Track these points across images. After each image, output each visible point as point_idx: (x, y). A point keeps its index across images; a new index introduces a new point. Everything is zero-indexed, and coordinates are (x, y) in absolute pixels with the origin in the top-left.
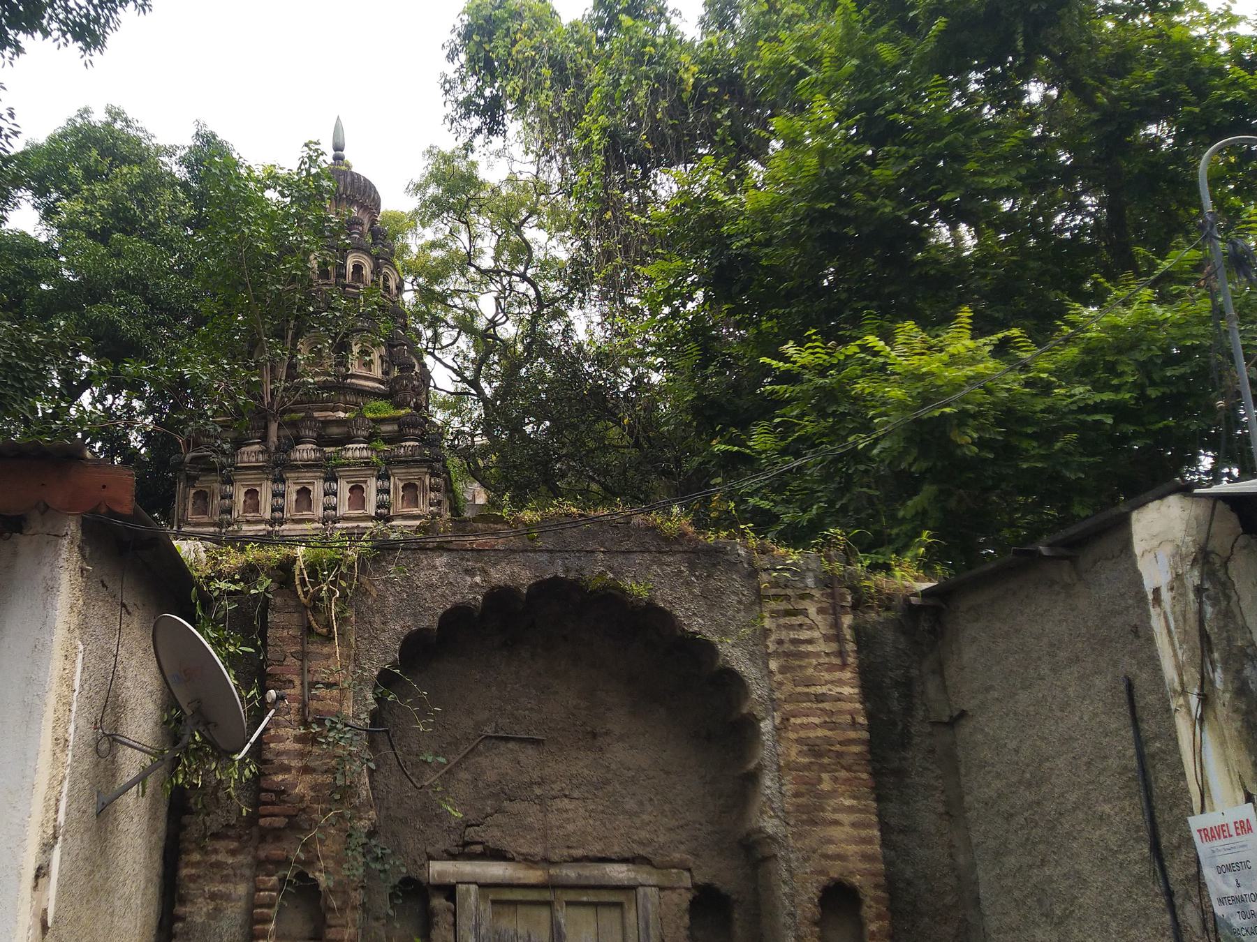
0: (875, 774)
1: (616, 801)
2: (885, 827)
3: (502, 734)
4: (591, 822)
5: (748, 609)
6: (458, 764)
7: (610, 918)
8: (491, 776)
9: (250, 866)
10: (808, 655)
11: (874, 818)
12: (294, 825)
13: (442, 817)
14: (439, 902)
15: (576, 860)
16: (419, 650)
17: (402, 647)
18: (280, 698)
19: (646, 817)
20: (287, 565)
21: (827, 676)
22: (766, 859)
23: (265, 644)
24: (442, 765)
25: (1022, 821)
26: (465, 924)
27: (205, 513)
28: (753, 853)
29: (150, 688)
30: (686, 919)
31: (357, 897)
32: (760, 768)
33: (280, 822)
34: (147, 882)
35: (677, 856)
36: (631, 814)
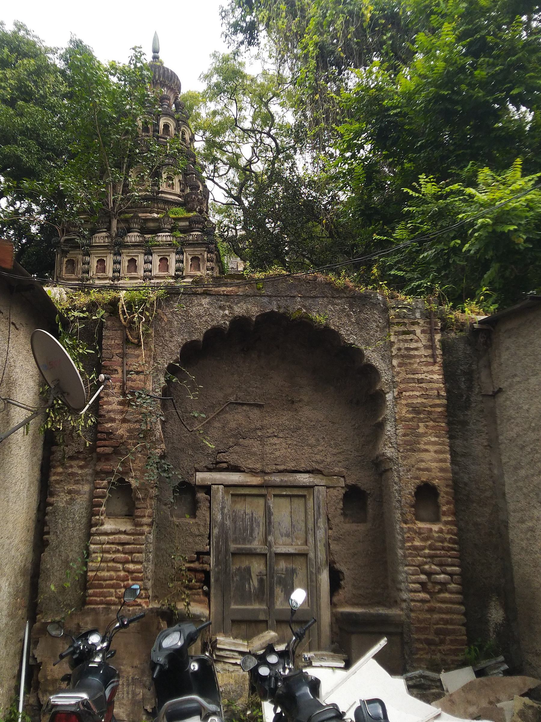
1: (304, 439)
2: (453, 453)
3: (239, 401)
4: (289, 450)
6: (214, 418)
7: (298, 503)
8: (233, 425)
9: (91, 475)
11: (448, 448)
12: (117, 452)
13: (204, 448)
14: (201, 495)
15: (280, 472)
16: (191, 353)
17: (181, 351)
18: (107, 379)
19: (320, 448)
20: (114, 302)
22: (386, 471)
23: (101, 348)
24: (204, 419)
26: (216, 508)
27: (73, 273)
28: (379, 467)
29: (31, 373)
30: (341, 505)
31: (154, 492)
32: (385, 420)
33: (108, 450)
34: (30, 484)
35: (337, 469)
36: (311, 446)
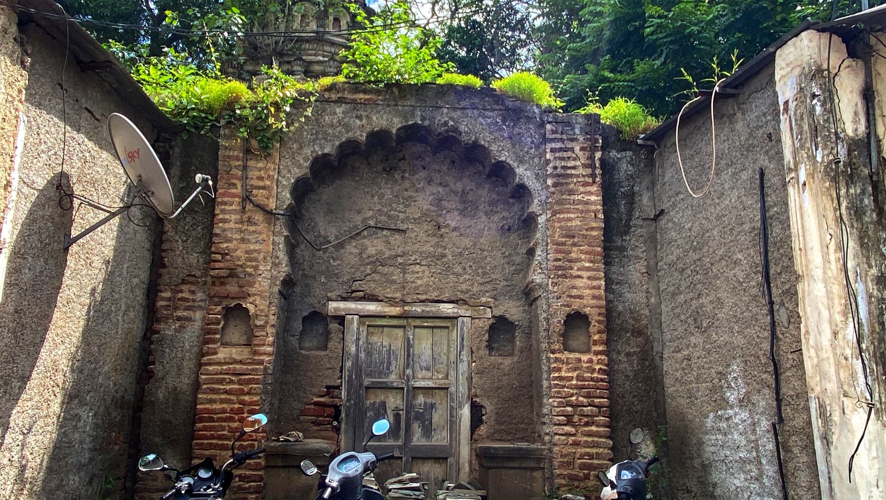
0: (605, 249)
5: (537, 147)
10: (572, 176)
21: (582, 189)
22: (536, 299)
25: (690, 272)
35: (484, 300)
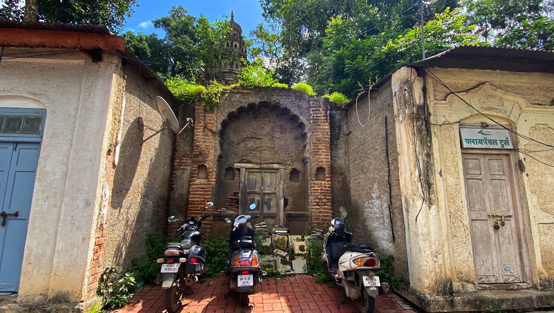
0: (330, 145)
2: (332, 156)
5: (307, 109)
28: (304, 161)
30: (289, 176)
35: (288, 163)
